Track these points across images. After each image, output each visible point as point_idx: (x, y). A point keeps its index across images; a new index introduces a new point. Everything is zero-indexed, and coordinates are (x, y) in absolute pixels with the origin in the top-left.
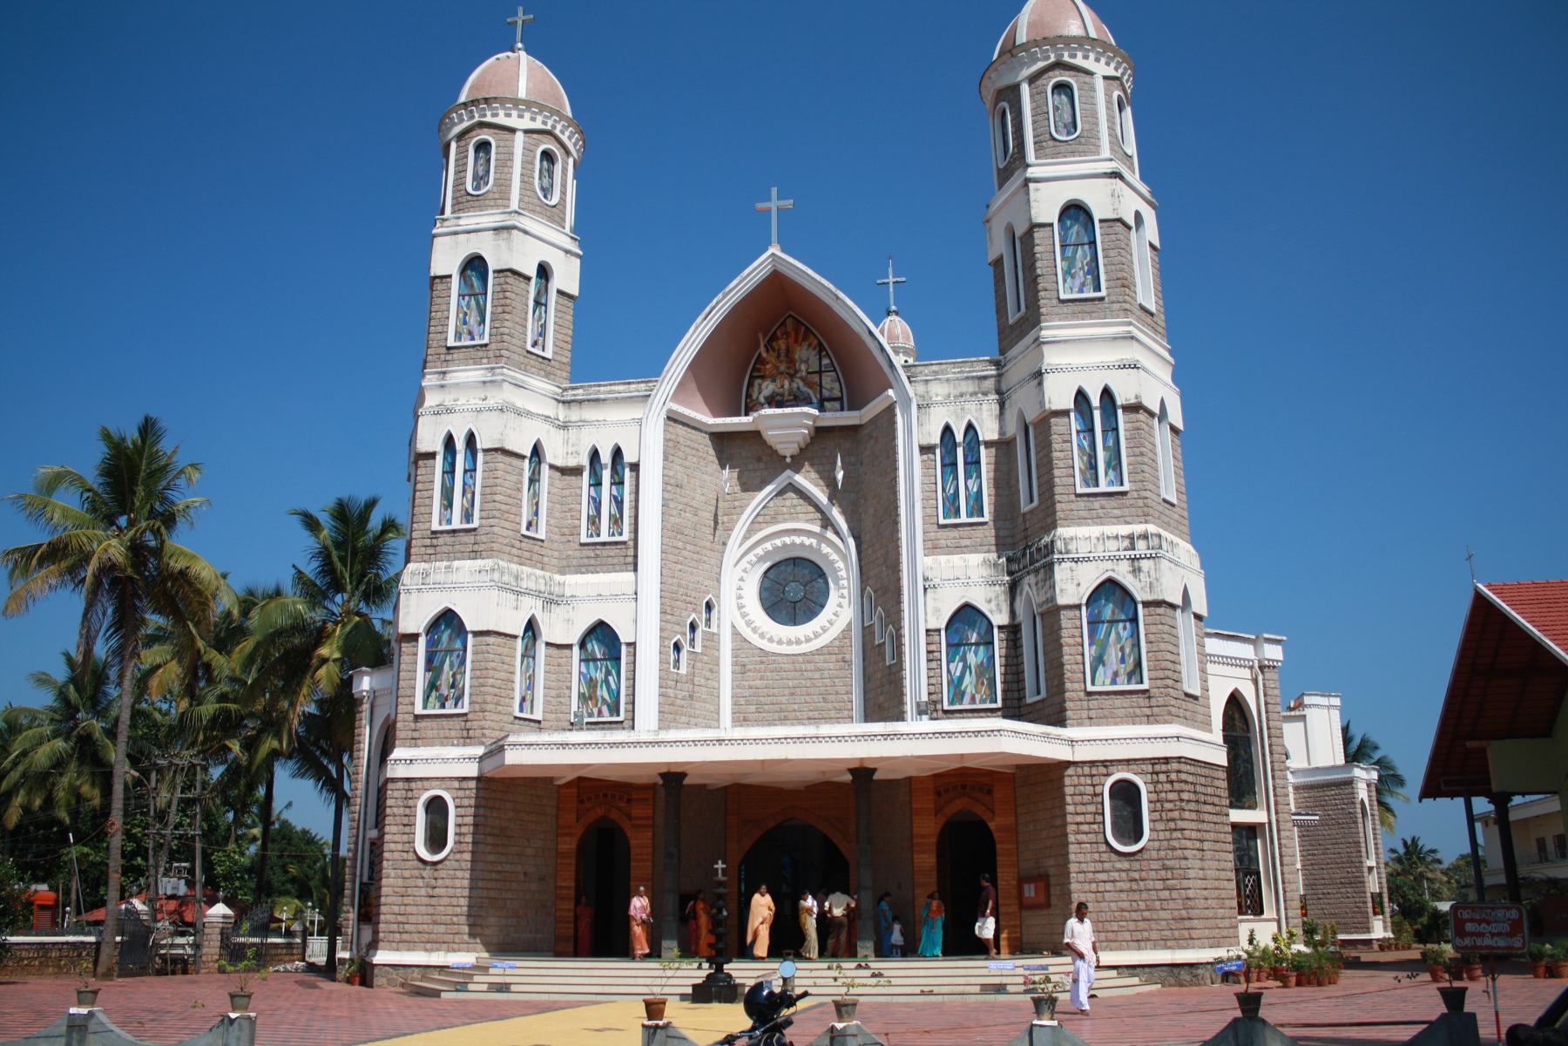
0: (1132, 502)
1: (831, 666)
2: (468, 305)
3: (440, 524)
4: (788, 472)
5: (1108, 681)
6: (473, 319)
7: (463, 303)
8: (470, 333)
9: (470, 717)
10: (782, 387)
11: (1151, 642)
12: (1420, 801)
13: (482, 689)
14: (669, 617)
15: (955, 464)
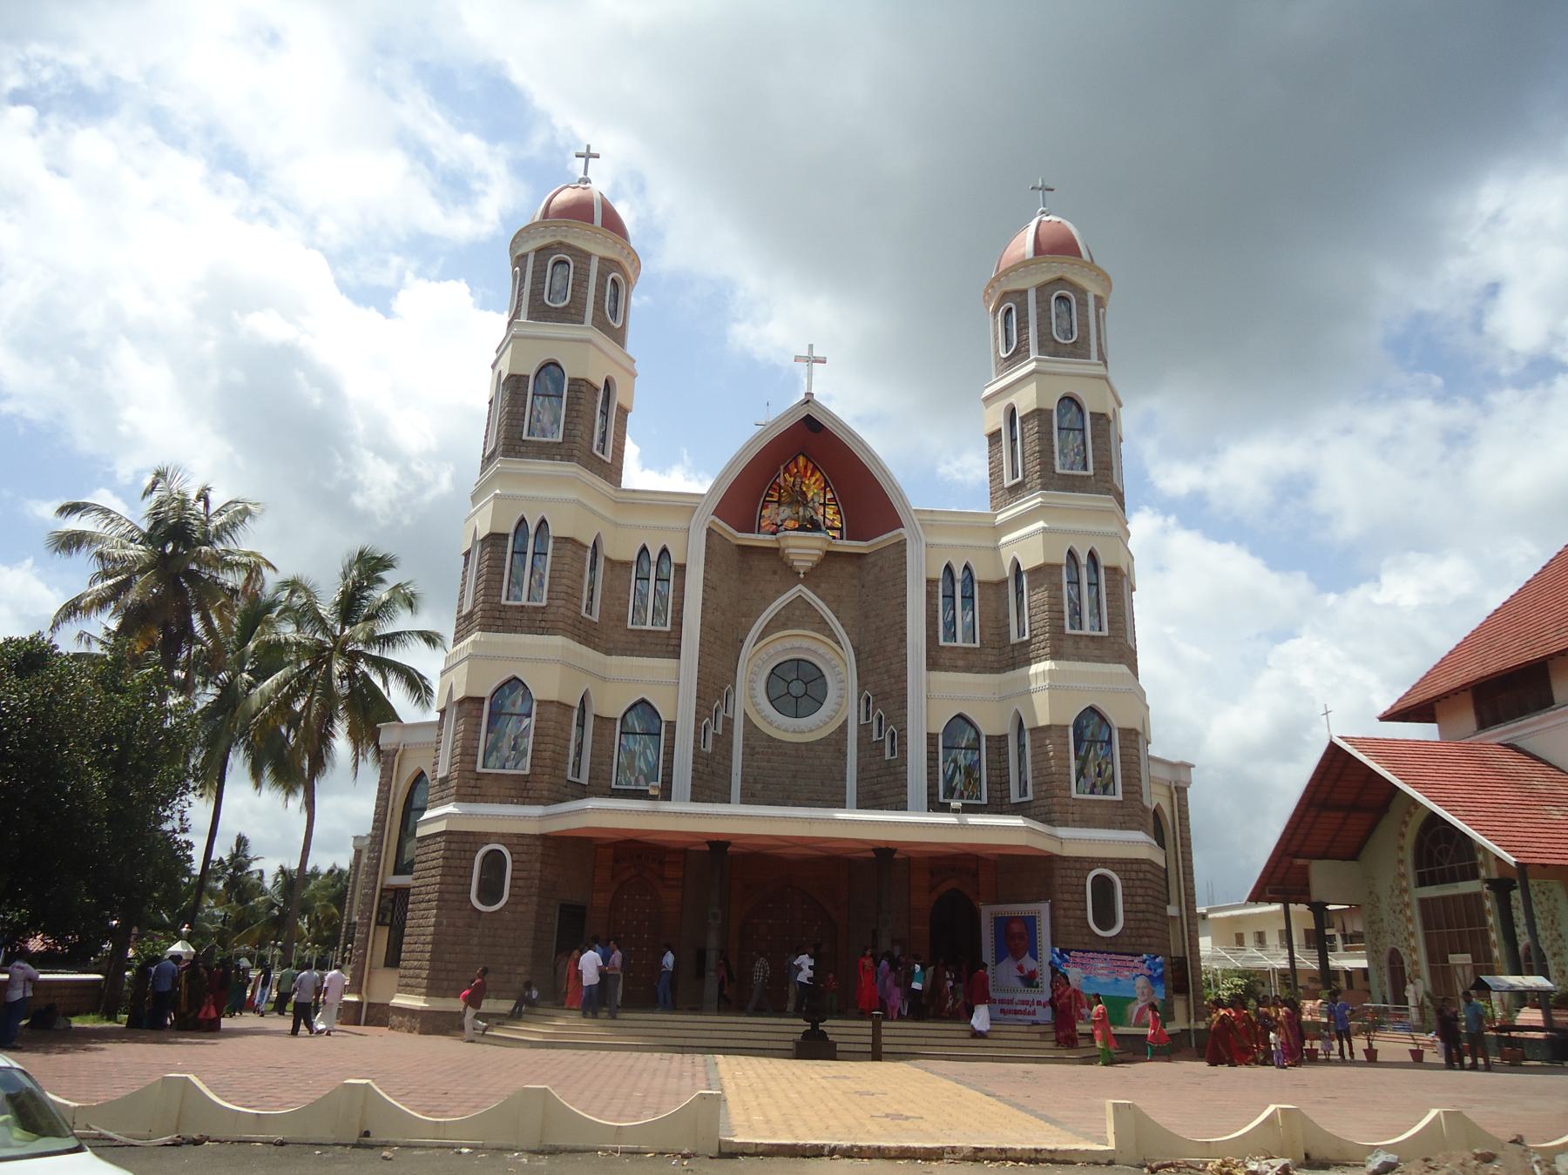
2: (542, 405)
4: (800, 586)
5: (1088, 790)
9: (530, 779)
10: (797, 513)
15: (953, 597)
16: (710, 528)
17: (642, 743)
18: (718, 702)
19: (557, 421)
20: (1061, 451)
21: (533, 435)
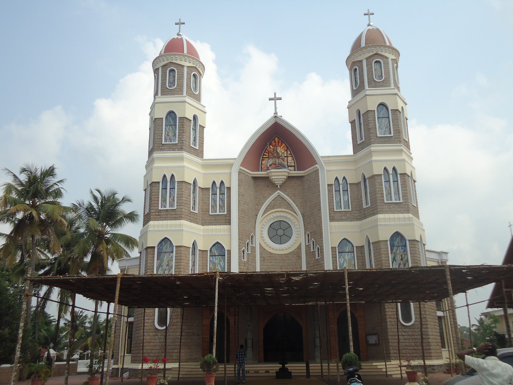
0: (403, 206)
2: (169, 129)
3: (161, 207)
4: (278, 191)
6: (171, 134)
7: (167, 128)
8: (170, 139)
10: (276, 162)
11: (412, 254)
12: (486, 309)
13: (179, 266)
14: (241, 241)
16: (239, 171)
17: (218, 259)
18: (248, 240)
19: (175, 135)
20: (379, 127)
21: (167, 142)
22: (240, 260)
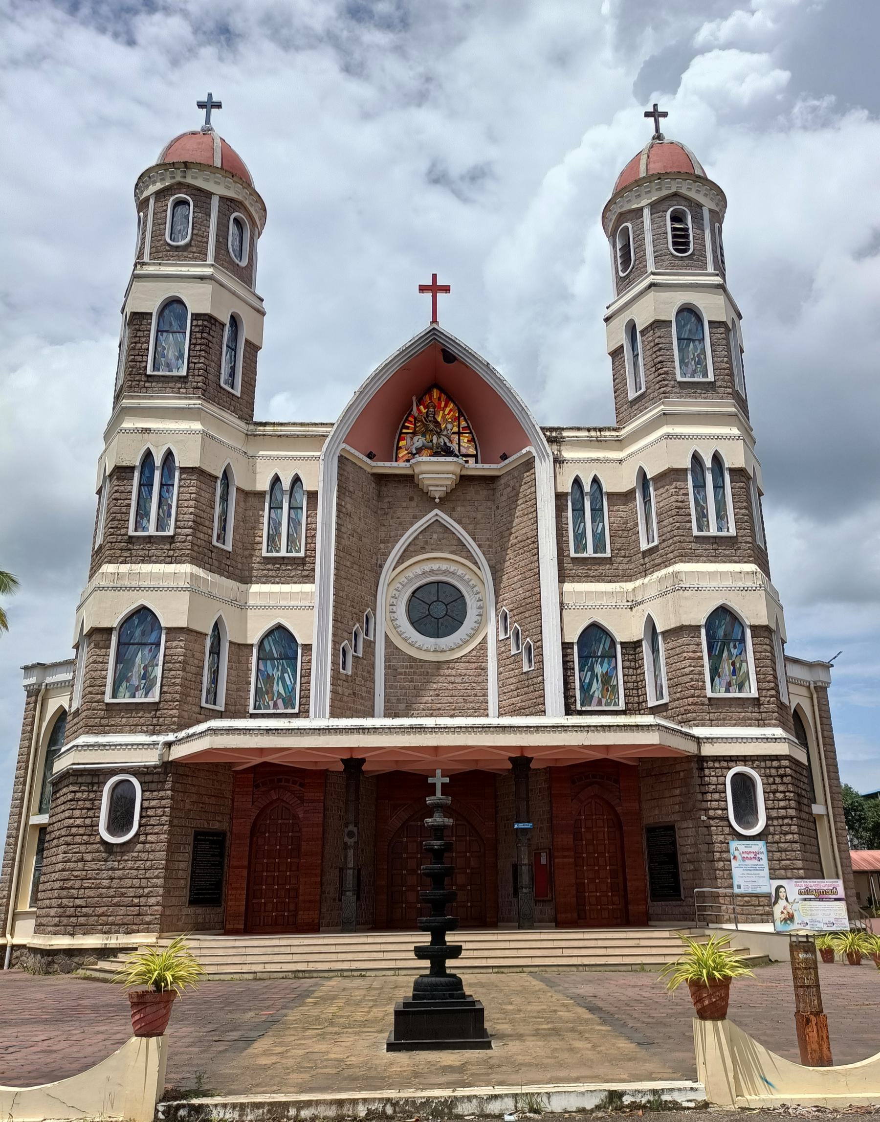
1: (471, 672)
4: (436, 511)
10: (431, 441)
16: (341, 456)
17: (280, 668)
18: (358, 625)
19: (181, 356)
20: (682, 361)
21: (159, 370)
22: (335, 671)
